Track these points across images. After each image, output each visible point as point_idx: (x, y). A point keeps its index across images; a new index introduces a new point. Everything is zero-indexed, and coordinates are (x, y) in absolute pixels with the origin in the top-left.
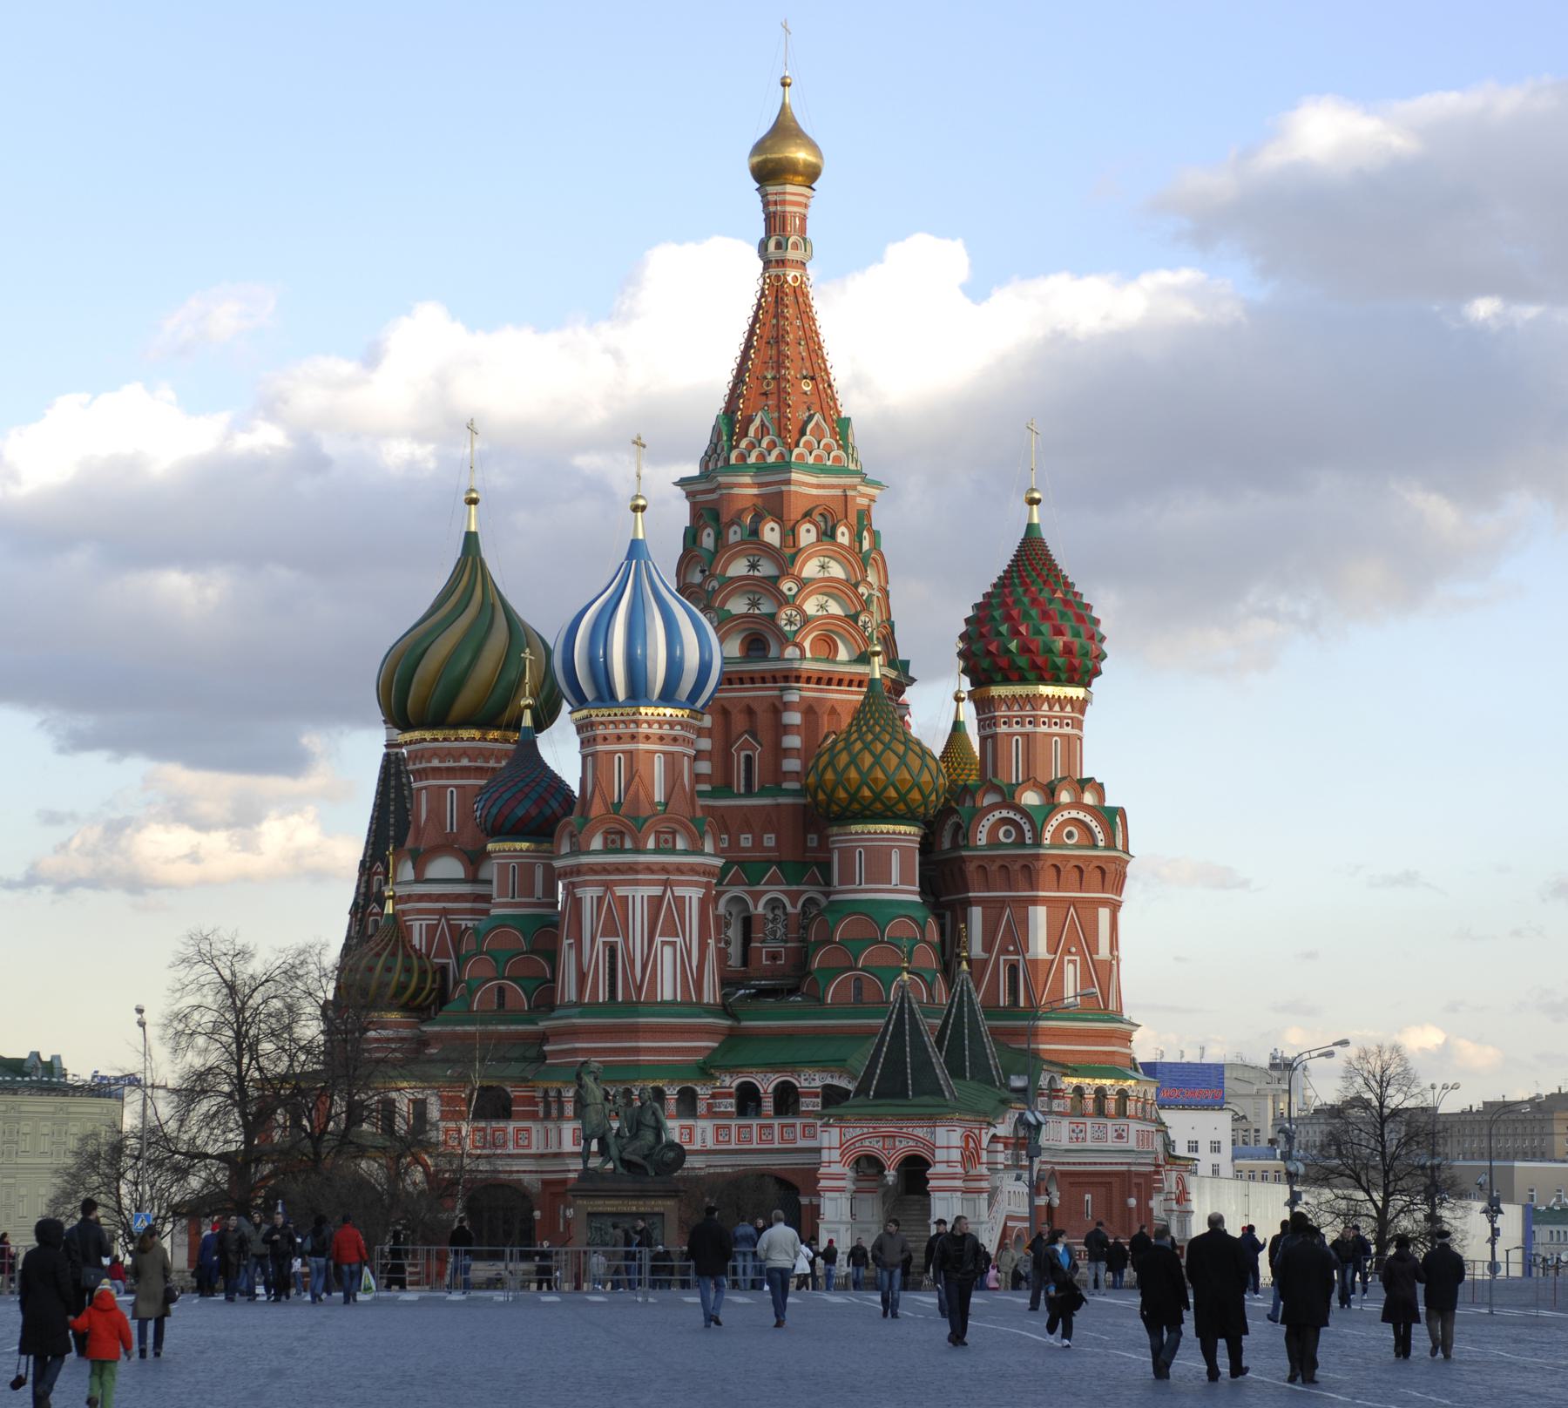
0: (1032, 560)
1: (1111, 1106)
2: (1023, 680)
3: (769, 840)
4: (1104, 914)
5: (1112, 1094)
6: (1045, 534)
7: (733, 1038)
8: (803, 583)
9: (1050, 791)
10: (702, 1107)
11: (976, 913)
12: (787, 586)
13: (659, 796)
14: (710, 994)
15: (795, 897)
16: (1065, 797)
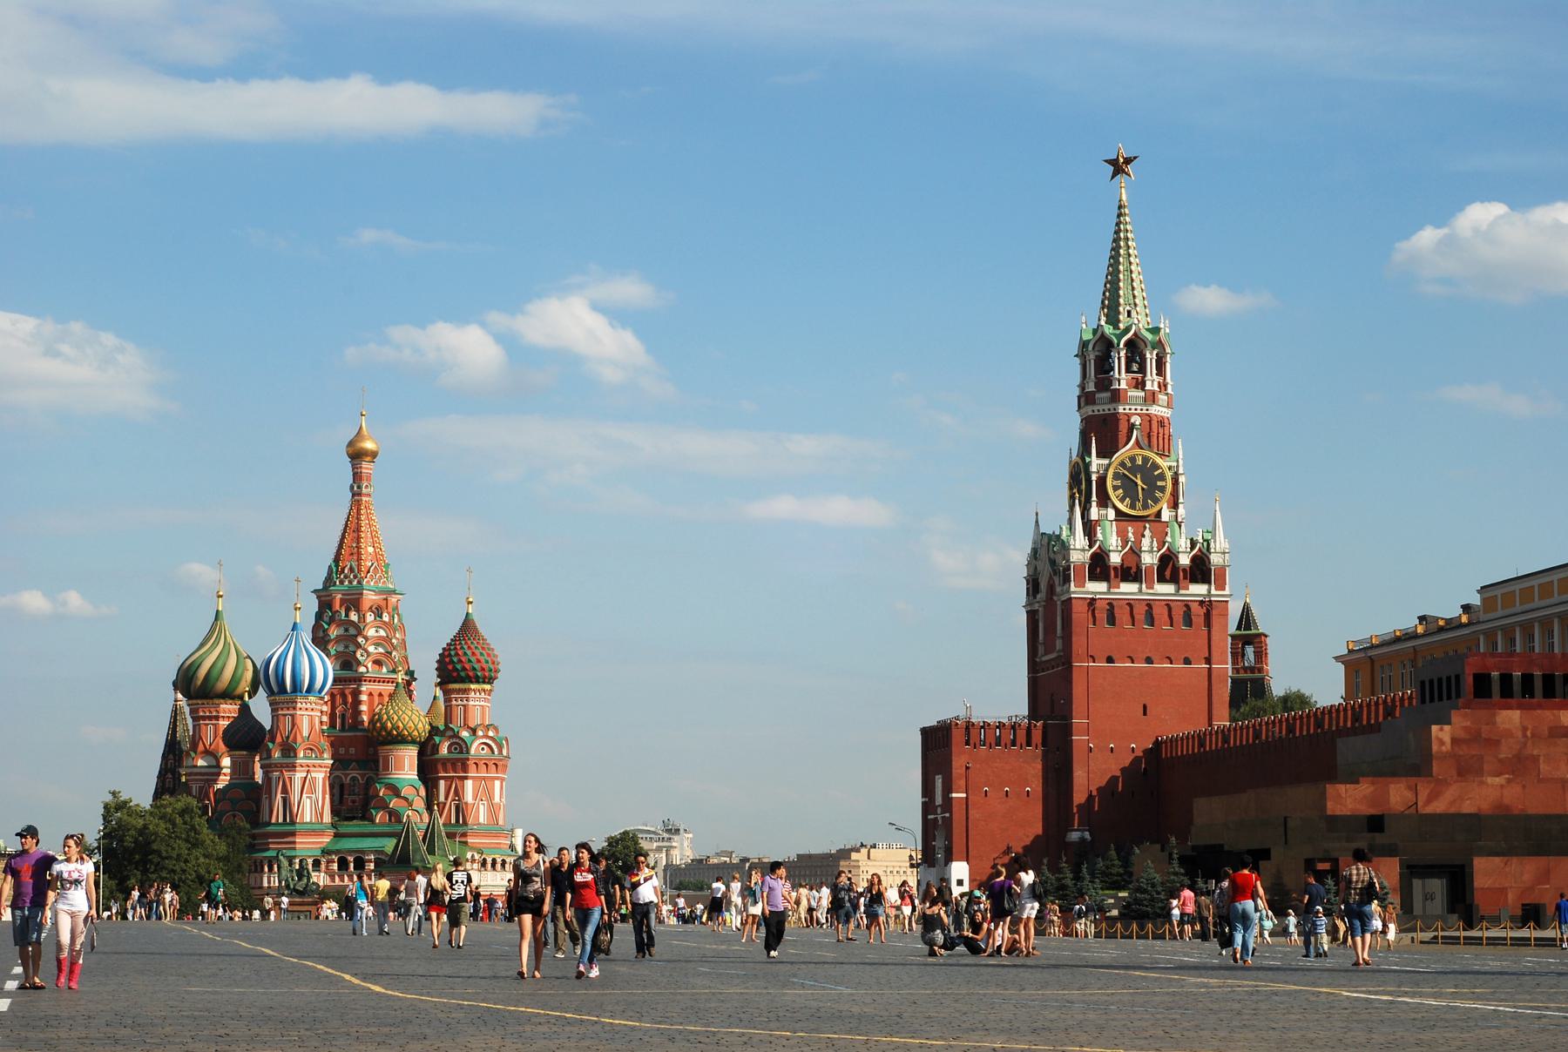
0: (468, 628)
1: (498, 866)
2: (462, 681)
3: (352, 751)
4: (497, 783)
5: (499, 860)
6: (476, 618)
7: (336, 835)
8: (366, 639)
9: (474, 731)
10: (323, 867)
11: (442, 783)
12: (360, 640)
13: (305, 734)
14: (327, 818)
15: (363, 776)
16: (480, 733)
